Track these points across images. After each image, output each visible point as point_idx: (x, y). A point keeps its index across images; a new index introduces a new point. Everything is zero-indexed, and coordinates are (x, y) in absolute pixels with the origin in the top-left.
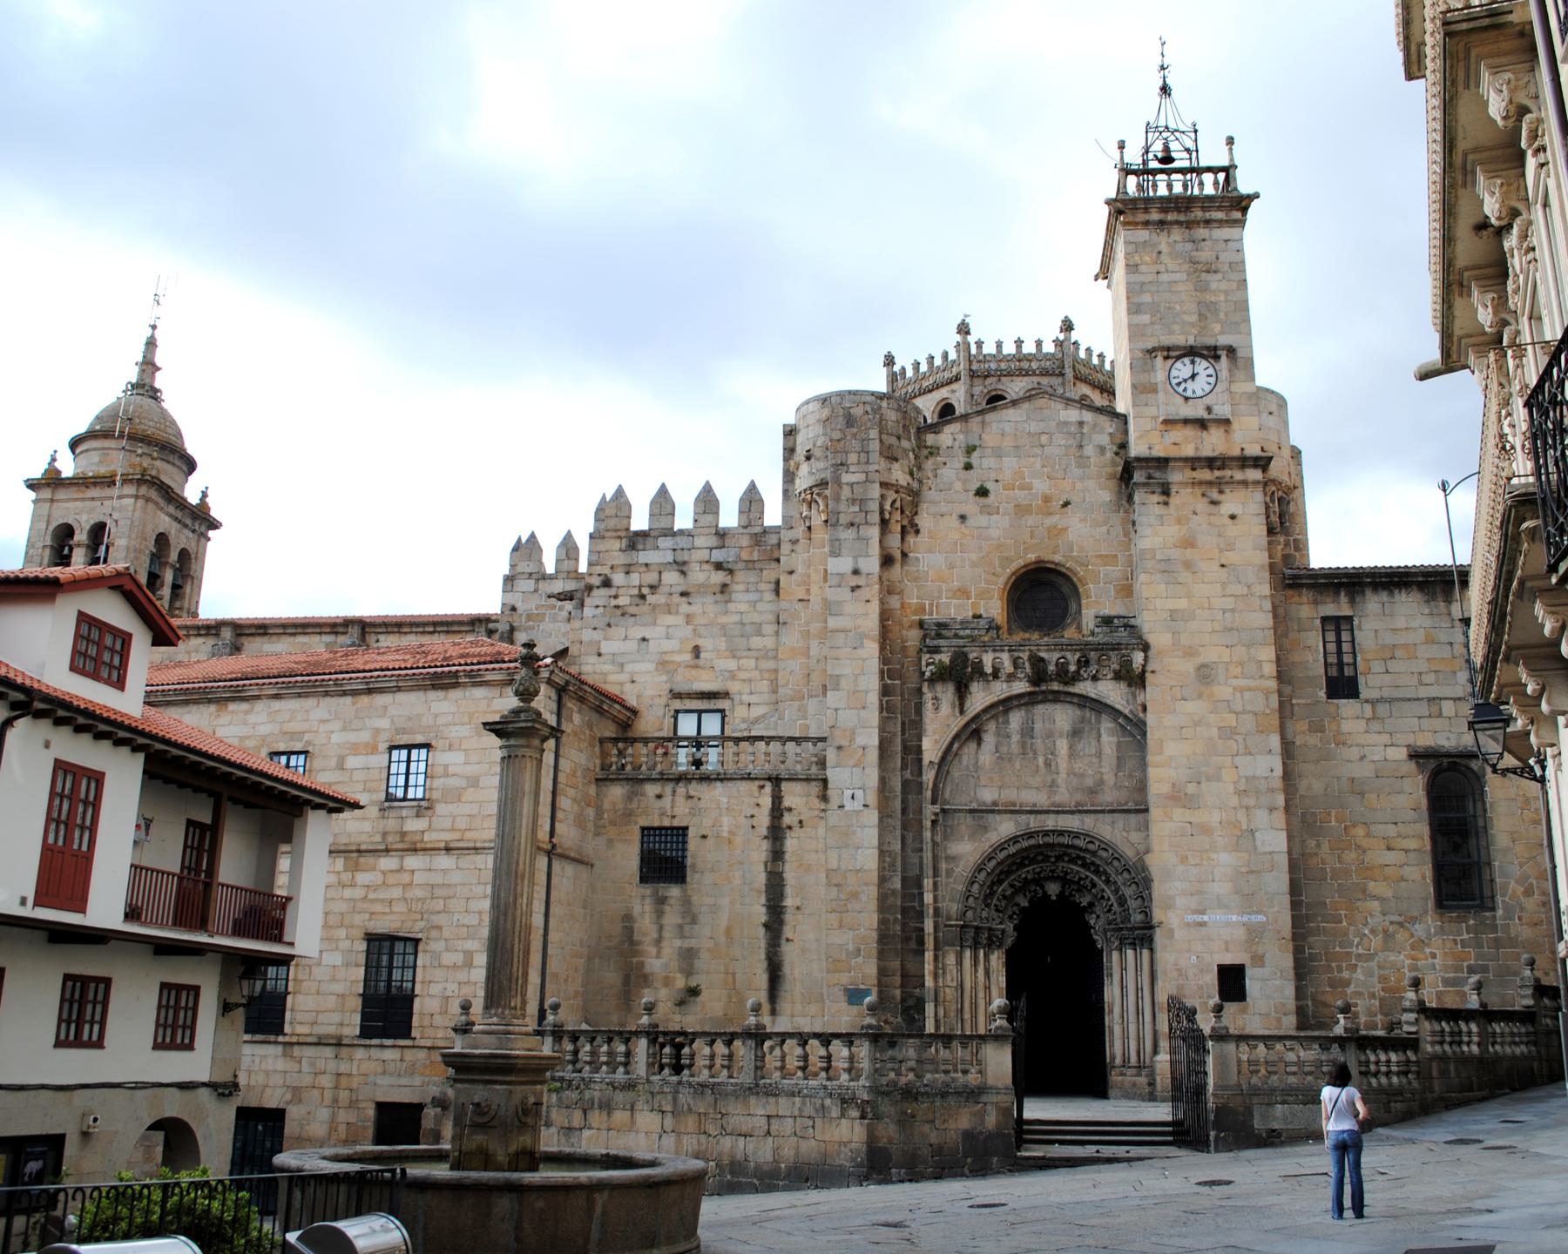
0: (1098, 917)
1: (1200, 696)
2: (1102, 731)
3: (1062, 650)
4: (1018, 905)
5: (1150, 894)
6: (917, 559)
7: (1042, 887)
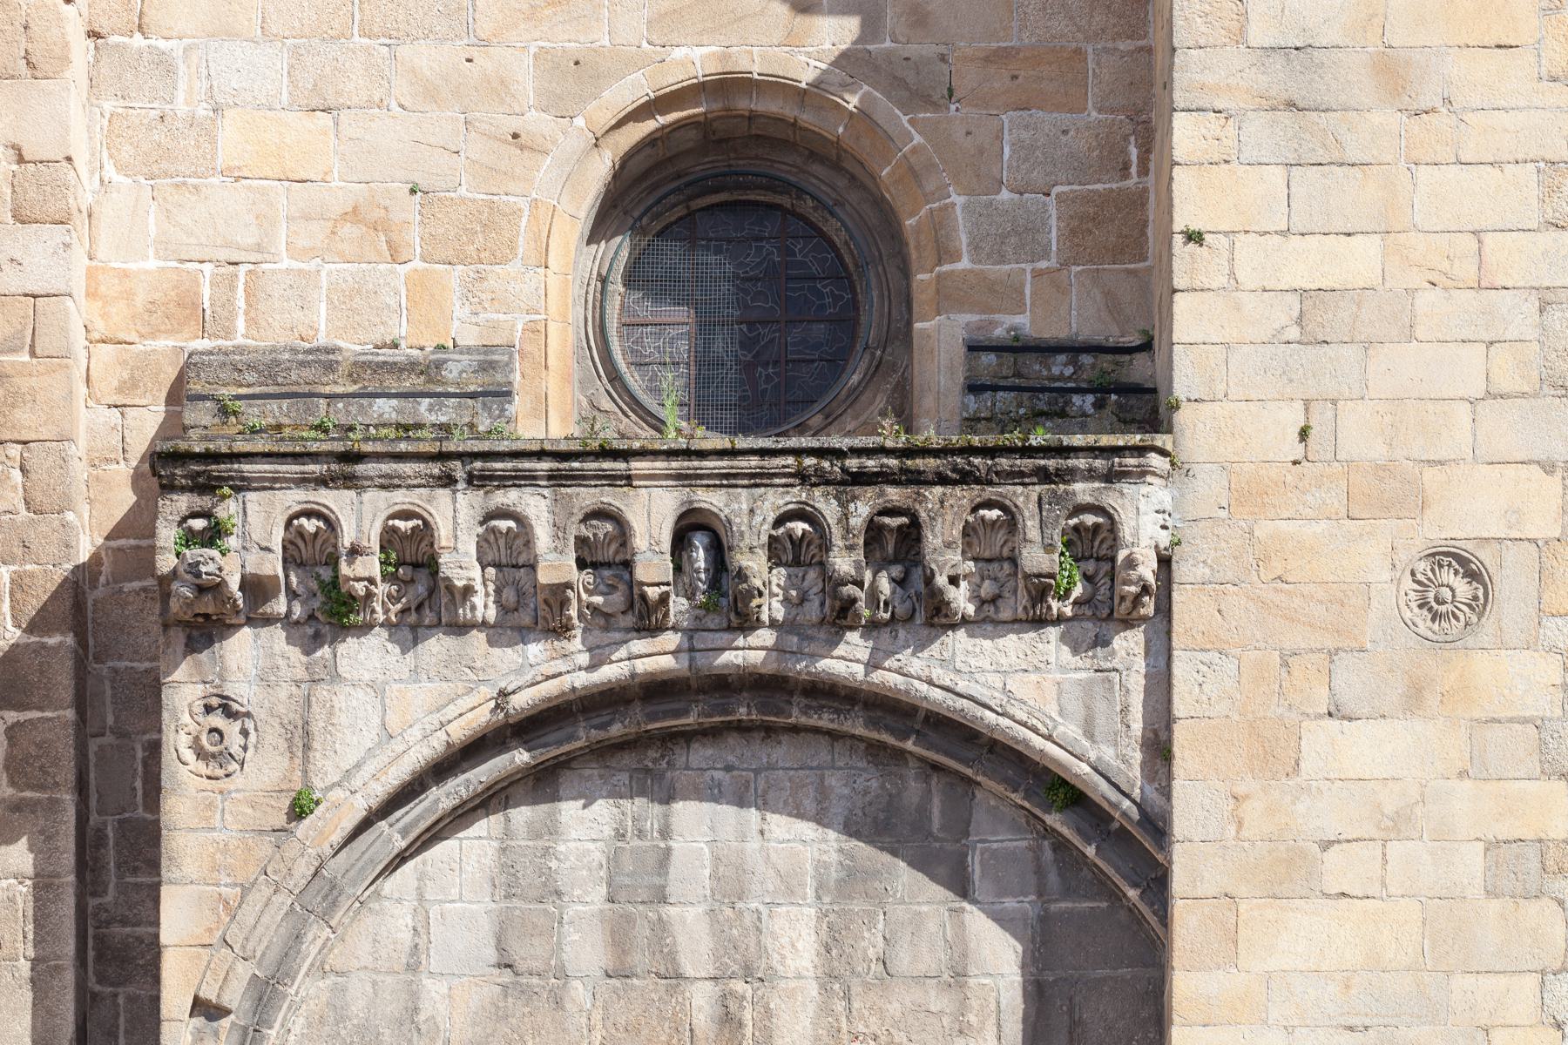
1: (1414, 698)
6: (165, 65)
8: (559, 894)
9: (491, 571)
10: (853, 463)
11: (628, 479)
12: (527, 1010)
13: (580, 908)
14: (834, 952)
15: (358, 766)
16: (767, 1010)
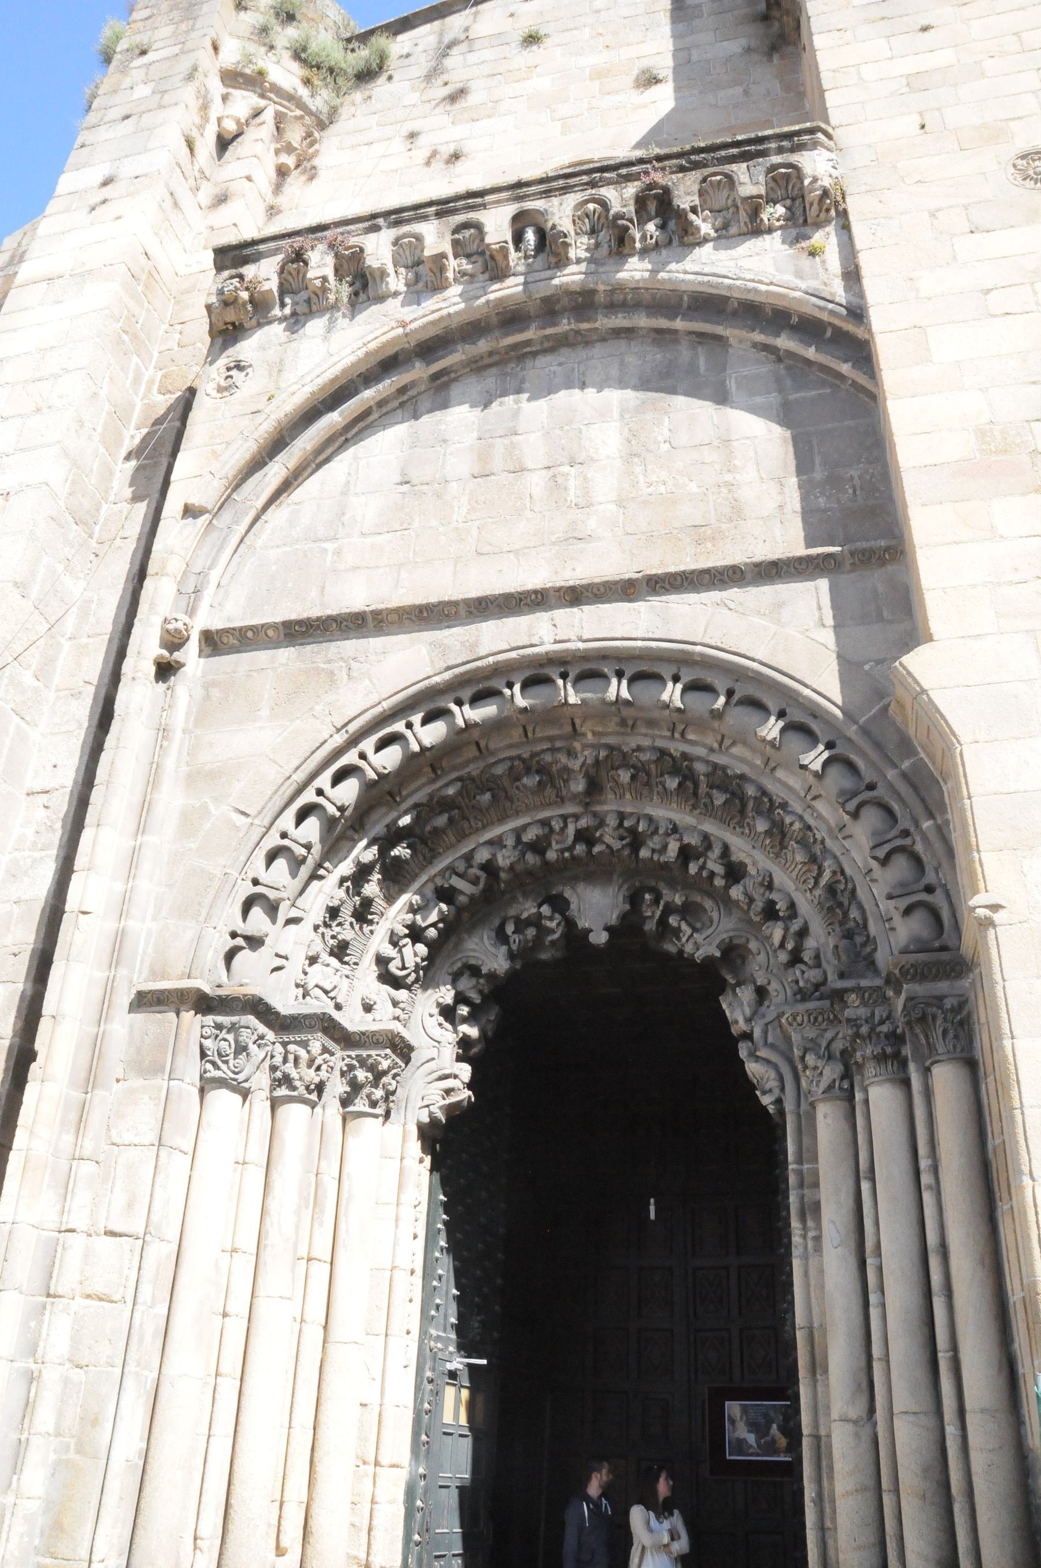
0: (761, 993)
2: (732, 385)
3: (593, 184)
4: (474, 971)
5: (943, 832)
7: (560, 904)
8: (445, 441)
9: (402, 270)
10: (624, 171)
11: (484, 206)
12: (416, 503)
13: (457, 445)
14: (633, 442)
15: (309, 373)
16: (585, 478)
